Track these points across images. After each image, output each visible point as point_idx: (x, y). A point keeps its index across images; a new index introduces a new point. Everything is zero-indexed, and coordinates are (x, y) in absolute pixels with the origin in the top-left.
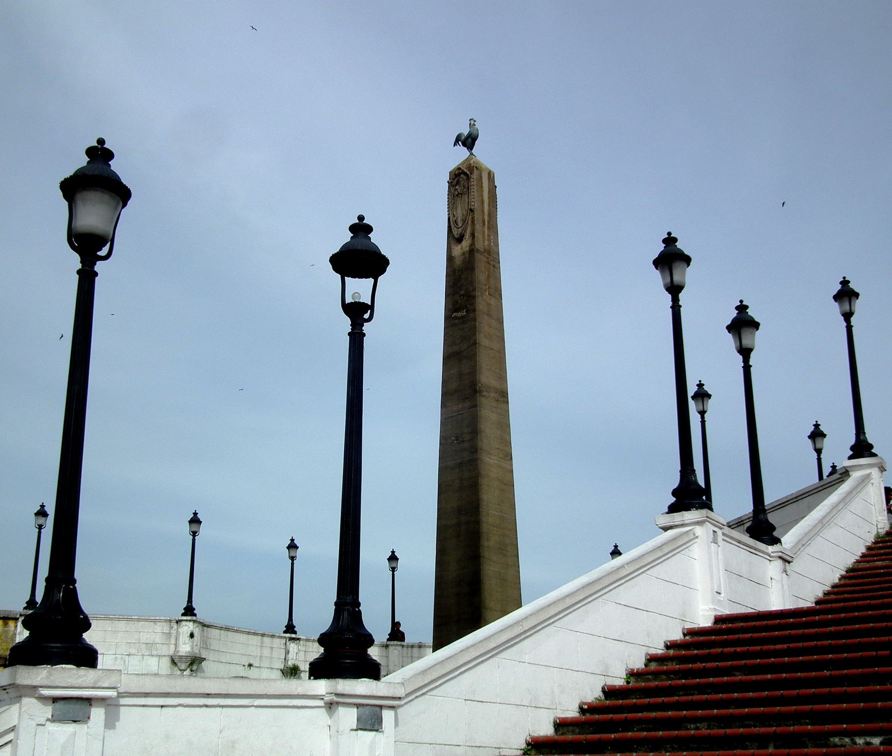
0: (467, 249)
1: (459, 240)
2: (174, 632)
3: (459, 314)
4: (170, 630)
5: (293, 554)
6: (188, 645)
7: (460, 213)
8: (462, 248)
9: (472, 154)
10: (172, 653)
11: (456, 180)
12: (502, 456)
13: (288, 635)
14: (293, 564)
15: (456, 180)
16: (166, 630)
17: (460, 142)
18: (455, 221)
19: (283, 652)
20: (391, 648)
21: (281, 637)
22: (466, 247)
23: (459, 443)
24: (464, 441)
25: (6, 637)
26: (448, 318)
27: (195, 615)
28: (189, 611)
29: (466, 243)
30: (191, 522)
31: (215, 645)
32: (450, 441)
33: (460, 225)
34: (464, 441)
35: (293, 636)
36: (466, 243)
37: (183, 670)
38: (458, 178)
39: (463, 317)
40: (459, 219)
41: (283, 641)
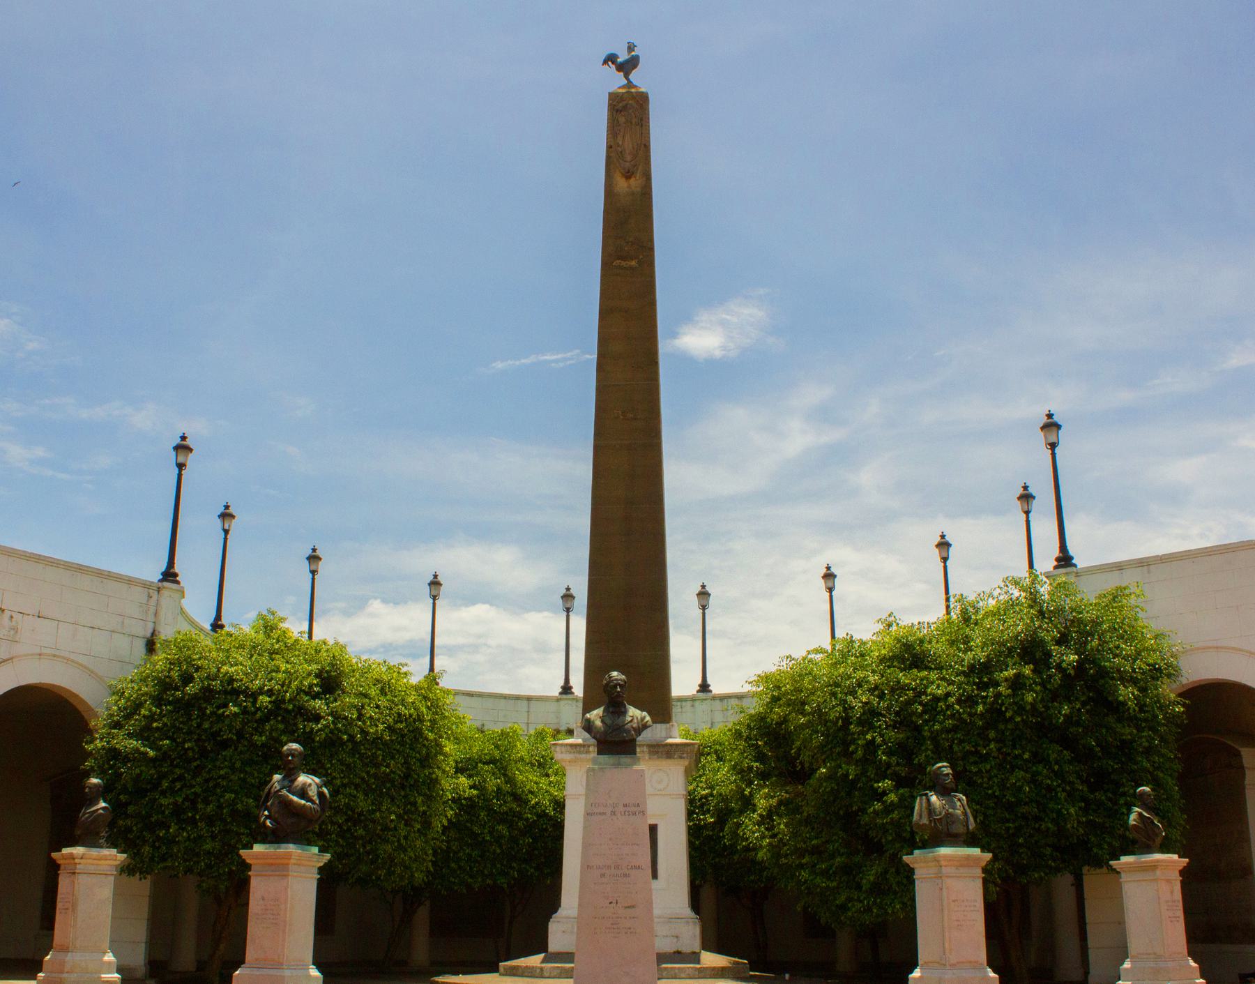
0: (639, 189)
1: (628, 175)
2: (153, 602)
3: (623, 263)
4: (148, 601)
5: (226, 527)
7: (628, 144)
8: (629, 187)
9: (630, 84)
10: (149, 635)
11: (621, 105)
15: (621, 105)
16: (144, 599)
17: (610, 63)
18: (621, 152)
22: (636, 187)
26: (606, 265)
27: (178, 583)
28: (170, 575)
29: (635, 183)
33: (629, 158)
36: (635, 183)
38: (625, 102)
39: (631, 268)
40: (627, 152)
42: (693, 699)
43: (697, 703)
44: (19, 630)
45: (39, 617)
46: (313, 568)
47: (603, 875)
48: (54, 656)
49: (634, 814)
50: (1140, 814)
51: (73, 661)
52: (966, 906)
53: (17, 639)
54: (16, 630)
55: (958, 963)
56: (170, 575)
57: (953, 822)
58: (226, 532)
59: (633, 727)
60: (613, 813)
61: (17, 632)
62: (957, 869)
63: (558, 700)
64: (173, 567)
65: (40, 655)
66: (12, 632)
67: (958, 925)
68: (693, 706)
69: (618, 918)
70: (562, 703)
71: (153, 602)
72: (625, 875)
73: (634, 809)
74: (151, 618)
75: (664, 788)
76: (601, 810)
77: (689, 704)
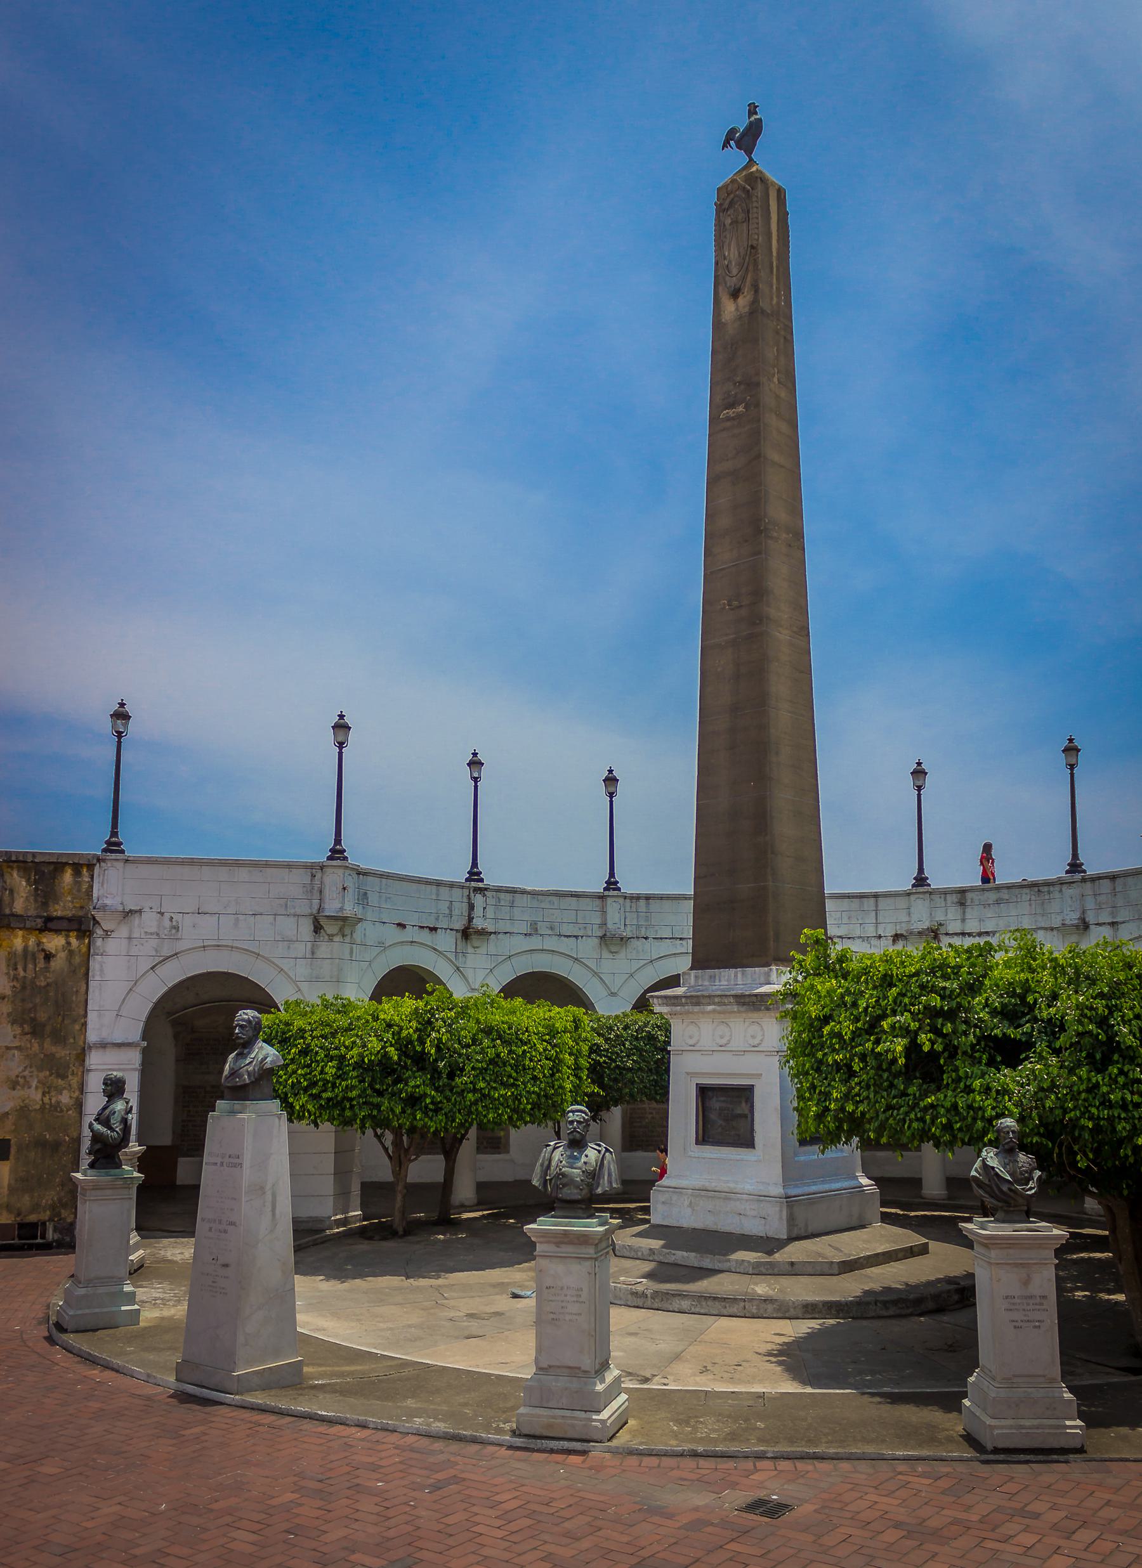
4: (311, 881)
5: (476, 775)
6: (337, 901)
12: (795, 629)
13: (473, 884)
14: (476, 787)
16: (307, 880)
19: (465, 906)
20: (609, 900)
21: (463, 887)
23: (732, 609)
24: (741, 606)
25: (79, 890)
27: (345, 858)
28: (337, 853)
30: (336, 727)
31: (373, 898)
32: (719, 607)
34: (741, 606)
35: (480, 885)
37: (333, 935)
41: (466, 892)
42: (1061, 882)
43: (1064, 887)
44: (180, 928)
45: (199, 913)
46: (611, 790)
47: (210, 1229)
48: (218, 946)
49: (235, 1166)
50: (983, 1161)
51: (237, 948)
52: (566, 1296)
53: (179, 937)
54: (177, 928)
55: (550, 1367)
56: (337, 853)
57: (564, 1185)
58: (476, 780)
59: (247, 1071)
60: (222, 1164)
61: (178, 931)
62: (558, 1247)
63: (909, 894)
64: (340, 844)
65: (204, 947)
66: (174, 931)
67: (553, 1319)
68: (1061, 891)
69: (217, 1276)
70: (913, 897)
71: (317, 881)
72: (225, 1232)
73: (236, 1161)
74: (316, 895)
75: (759, 1044)
76: (213, 1160)
77: (1057, 888)
